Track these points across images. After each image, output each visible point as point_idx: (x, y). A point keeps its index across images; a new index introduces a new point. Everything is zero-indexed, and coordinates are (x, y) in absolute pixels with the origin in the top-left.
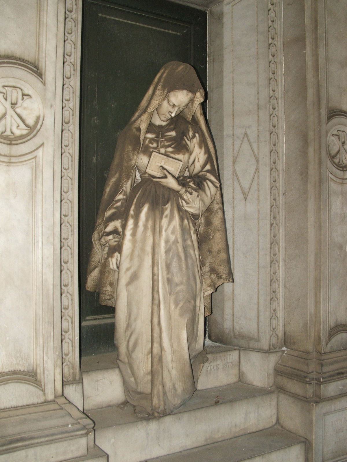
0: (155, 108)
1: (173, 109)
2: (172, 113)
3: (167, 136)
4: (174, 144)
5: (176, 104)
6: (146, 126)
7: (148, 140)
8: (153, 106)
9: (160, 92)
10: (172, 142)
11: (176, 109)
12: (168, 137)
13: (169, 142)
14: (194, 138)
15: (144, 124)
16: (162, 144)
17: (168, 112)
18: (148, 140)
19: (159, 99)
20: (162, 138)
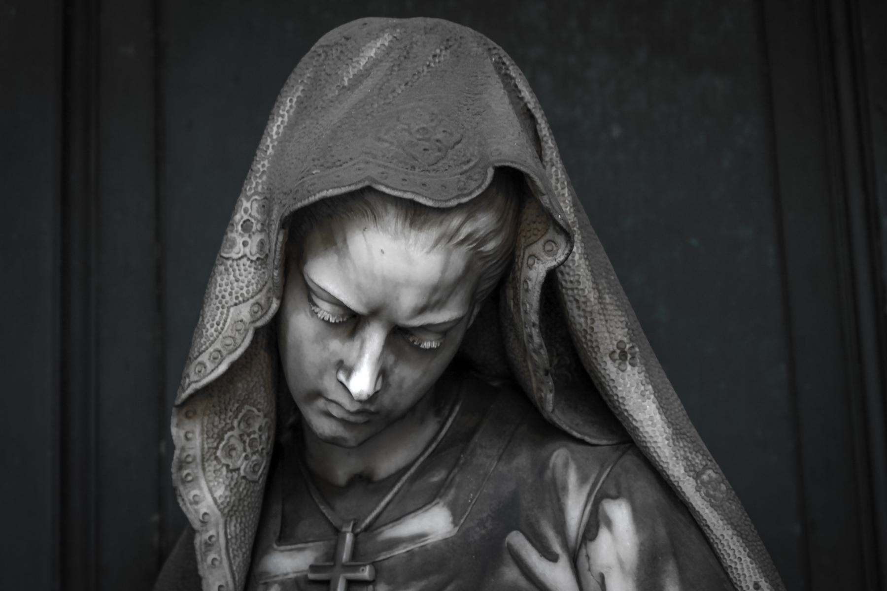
0: (231, 352)
1: (357, 343)
2: (350, 372)
6: (220, 492)
8: (218, 345)
9: (257, 238)
12: (400, 551)
15: (203, 483)
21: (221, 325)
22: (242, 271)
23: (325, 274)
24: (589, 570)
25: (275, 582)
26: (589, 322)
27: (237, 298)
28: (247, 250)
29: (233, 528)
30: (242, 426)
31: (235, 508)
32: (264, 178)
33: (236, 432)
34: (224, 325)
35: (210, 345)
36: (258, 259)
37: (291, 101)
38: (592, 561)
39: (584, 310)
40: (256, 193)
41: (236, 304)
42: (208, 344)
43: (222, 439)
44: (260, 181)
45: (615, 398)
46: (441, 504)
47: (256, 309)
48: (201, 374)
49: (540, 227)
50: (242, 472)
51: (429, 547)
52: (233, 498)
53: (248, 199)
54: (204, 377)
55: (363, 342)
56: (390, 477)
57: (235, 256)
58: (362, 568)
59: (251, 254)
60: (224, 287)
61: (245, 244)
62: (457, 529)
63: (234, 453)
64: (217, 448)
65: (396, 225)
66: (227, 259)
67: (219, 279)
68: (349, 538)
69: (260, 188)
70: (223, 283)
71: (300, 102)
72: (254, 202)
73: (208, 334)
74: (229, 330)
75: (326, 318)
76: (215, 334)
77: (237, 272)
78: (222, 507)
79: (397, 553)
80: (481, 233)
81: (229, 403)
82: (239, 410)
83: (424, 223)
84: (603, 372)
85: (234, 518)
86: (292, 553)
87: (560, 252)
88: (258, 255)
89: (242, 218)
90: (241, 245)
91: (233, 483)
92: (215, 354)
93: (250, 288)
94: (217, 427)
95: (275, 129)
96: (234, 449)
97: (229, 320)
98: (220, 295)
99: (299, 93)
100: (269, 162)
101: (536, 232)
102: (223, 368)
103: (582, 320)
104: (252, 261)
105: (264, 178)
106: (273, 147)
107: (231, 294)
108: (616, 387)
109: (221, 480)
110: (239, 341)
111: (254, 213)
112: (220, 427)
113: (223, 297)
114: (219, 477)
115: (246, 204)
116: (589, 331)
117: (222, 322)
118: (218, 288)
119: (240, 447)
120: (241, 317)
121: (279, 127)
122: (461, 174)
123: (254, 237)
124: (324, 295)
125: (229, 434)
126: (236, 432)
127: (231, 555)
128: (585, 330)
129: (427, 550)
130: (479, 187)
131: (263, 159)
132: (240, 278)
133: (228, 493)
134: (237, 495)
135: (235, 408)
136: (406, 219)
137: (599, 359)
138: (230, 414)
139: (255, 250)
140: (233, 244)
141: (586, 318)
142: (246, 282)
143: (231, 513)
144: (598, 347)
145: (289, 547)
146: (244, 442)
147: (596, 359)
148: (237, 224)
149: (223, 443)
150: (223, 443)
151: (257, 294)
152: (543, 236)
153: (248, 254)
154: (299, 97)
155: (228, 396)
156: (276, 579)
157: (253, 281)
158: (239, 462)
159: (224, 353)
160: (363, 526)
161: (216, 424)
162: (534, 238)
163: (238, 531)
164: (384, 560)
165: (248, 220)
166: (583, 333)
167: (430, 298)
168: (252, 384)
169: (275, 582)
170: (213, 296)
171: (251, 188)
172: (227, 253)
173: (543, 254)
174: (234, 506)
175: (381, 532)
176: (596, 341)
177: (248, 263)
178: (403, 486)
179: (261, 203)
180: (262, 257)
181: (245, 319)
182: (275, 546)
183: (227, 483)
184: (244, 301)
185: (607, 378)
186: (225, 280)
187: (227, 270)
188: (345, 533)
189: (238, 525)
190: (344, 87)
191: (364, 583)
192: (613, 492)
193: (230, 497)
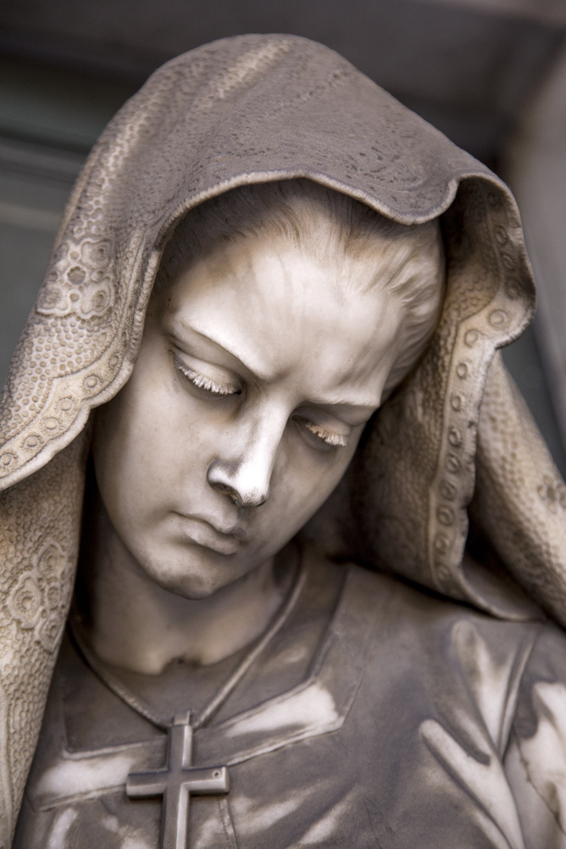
1: (244, 428)
2: (233, 466)
3: (255, 739)
4: (338, 810)
5: (255, 362)
7: (64, 823)
8: (35, 428)
9: (91, 292)
10: (308, 792)
11: (272, 416)
12: (265, 749)
13: (280, 795)
14: (531, 731)
16: (210, 827)
17: (202, 474)
18: (64, 823)
19: (87, 355)
20: (200, 765)
21: (40, 402)
22: (70, 333)
23: (213, 318)
24: (529, 779)
25: (68, 806)
26: (510, 446)
27: (62, 367)
28: (77, 306)
29: (17, 718)
30: (43, 566)
31: (23, 688)
32: (100, 217)
33: (34, 573)
34: (44, 402)
35: (23, 429)
36: (93, 318)
37: (131, 129)
38: (532, 767)
39: (503, 432)
40: (88, 235)
41: (61, 376)
42: (19, 426)
43: (15, 581)
44: (94, 221)
45: (544, 548)
46: (319, 684)
47: (91, 382)
48: (8, 467)
49: (479, 295)
50: (36, 633)
51: (307, 743)
52: (23, 672)
53: (77, 242)
54: (15, 470)
55: (256, 424)
56: (225, 660)
57: (57, 311)
58: (215, 772)
59: (83, 312)
60: (44, 351)
61: (74, 298)
62: (342, 719)
63: (28, 605)
64: (7, 593)
65: (328, 246)
66: (48, 316)
67: (35, 341)
68: (187, 732)
69: (93, 230)
70: (43, 346)
71: (144, 131)
72: (86, 246)
73: (20, 413)
74: (52, 409)
75: (207, 386)
76: (31, 413)
77: (63, 334)
78: (7, 682)
79: (259, 752)
80: (422, 282)
81: (29, 529)
82: (39, 542)
83: (363, 248)
84: (528, 514)
85: (20, 702)
86: (93, 761)
87: (514, 323)
88: (94, 313)
89: (69, 265)
90: (69, 300)
91: (24, 649)
92: (32, 441)
93: (82, 355)
94: (10, 560)
95: (111, 160)
96: (29, 598)
97: (51, 396)
98: (38, 362)
99: (142, 122)
100: (105, 199)
101: (474, 302)
102: (44, 458)
103: (499, 445)
104: (84, 321)
105: (100, 217)
106: (111, 181)
107: (53, 361)
108: (546, 533)
109: (9, 642)
110: (67, 424)
111: (86, 259)
112: (15, 561)
113: (43, 365)
114: (6, 637)
115: (74, 248)
116: (509, 458)
117: (41, 397)
118: (35, 353)
119: (37, 597)
120: (69, 392)
121: (116, 157)
122: (410, 190)
123: (86, 290)
124: (209, 352)
125: (26, 574)
126: (34, 573)
127: (12, 760)
128: (504, 459)
129: (305, 747)
130: (438, 205)
131: (98, 194)
132: (68, 342)
133: (16, 662)
134: (28, 668)
135: (37, 538)
136: (340, 240)
137: (523, 497)
138: (30, 544)
139: (88, 306)
140: (56, 298)
141: (505, 442)
142: (76, 347)
143: (18, 694)
144: (521, 480)
145: (89, 754)
146: (43, 590)
147: (517, 496)
148: (62, 273)
149: (17, 587)
150: (17, 587)
151: (92, 363)
152: (485, 306)
153: (78, 311)
154: (141, 126)
155: (29, 517)
156: (69, 801)
157: (86, 346)
158: (35, 619)
159: (45, 438)
160: (203, 718)
161: (10, 556)
162: (473, 309)
163: (23, 724)
164: (240, 763)
165: (78, 268)
166: (500, 462)
167: (356, 361)
168: (60, 507)
169: (68, 806)
170: (26, 364)
171: (80, 229)
172: (47, 309)
173: (487, 327)
174: (22, 683)
175: (231, 726)
176: (520, 471)
177: (79, 323)
178: (249, 667)
179: (96, 247)
180: (101, 314)
181: (74, 396)
182: (66, 754)
183: (17, 647)
184: (73, 373)
185: (534, 521)
186: (45, 343)
187: (48, 330)
188: (181, 726)
189: (24, 715)
190: (219, 100)
191: (216, 795)
192: (545, 673)
193: (19, 668)
